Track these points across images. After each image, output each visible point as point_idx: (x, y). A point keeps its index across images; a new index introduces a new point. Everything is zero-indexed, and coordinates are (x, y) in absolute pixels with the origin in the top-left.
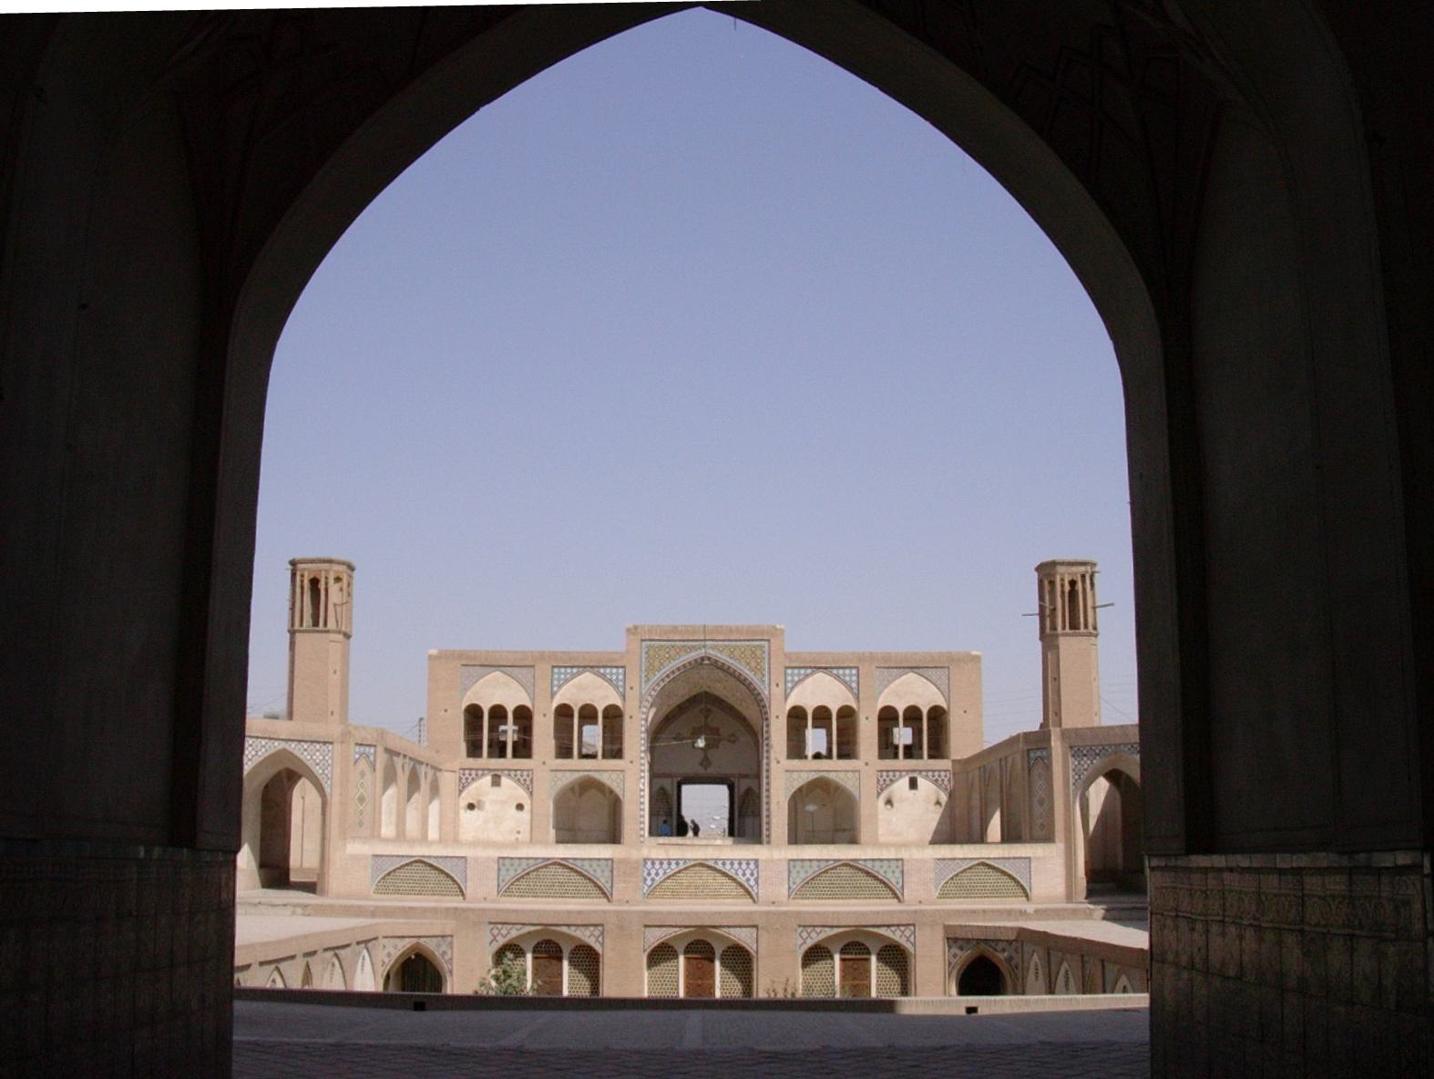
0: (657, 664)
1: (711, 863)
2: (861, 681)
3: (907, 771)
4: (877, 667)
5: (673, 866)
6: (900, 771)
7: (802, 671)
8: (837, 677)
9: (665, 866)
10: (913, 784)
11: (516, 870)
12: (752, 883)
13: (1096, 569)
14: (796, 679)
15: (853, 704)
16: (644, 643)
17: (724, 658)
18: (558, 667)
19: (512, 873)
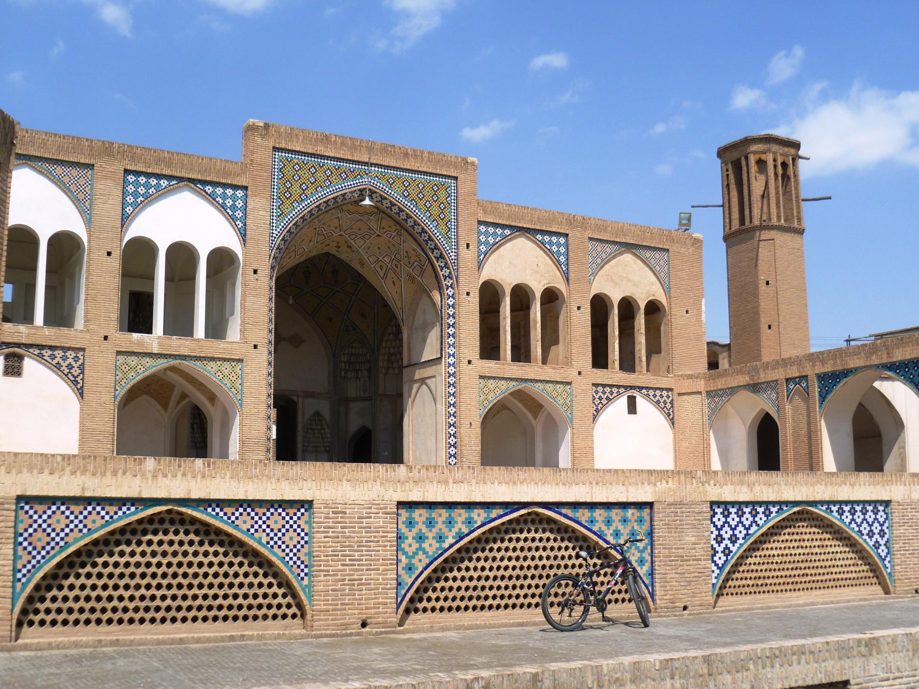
0: (296, 190)
1: (820, 511)
2: (571, 254)
3: (627, 388)
4: (590, 238)
5: (761, 519)
6: (619, 387)
7: (499, 231)
8: (541, 245)
9: (747, 519)
10: (632, 408)
11: (440, 538)
12: (883, 551)
13: (801, 153)
14: (491, 240)
15: (561, 286)
16: (278, 154)
17: (395, 194)
18: (138, 173)
19: (431, 546)
